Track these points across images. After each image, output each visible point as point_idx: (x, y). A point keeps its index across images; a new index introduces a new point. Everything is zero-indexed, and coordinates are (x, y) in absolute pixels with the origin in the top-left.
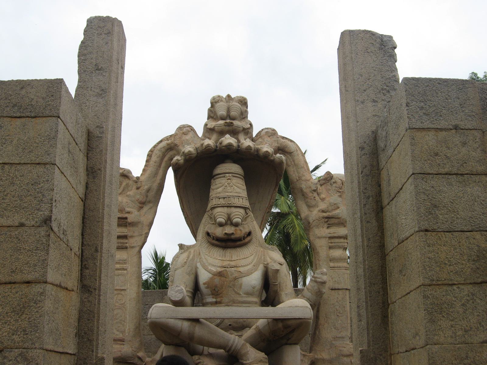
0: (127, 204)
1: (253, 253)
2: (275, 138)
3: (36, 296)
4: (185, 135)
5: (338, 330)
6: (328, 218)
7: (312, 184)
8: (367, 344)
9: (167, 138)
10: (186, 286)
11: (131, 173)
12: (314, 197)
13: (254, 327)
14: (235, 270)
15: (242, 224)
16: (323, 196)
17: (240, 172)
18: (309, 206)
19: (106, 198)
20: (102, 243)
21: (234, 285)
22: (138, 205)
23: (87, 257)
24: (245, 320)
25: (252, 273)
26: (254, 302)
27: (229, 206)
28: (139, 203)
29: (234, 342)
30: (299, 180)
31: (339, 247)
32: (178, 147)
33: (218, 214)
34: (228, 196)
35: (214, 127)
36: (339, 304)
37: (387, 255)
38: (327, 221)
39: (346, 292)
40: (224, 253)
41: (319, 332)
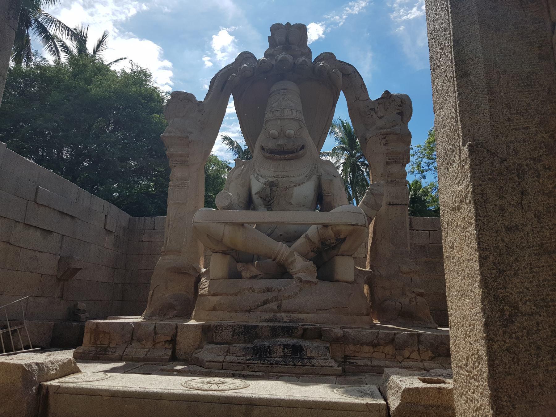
10: (239, 197)
13: (304, 235)
35: (273, 52)
38: (385, 138)
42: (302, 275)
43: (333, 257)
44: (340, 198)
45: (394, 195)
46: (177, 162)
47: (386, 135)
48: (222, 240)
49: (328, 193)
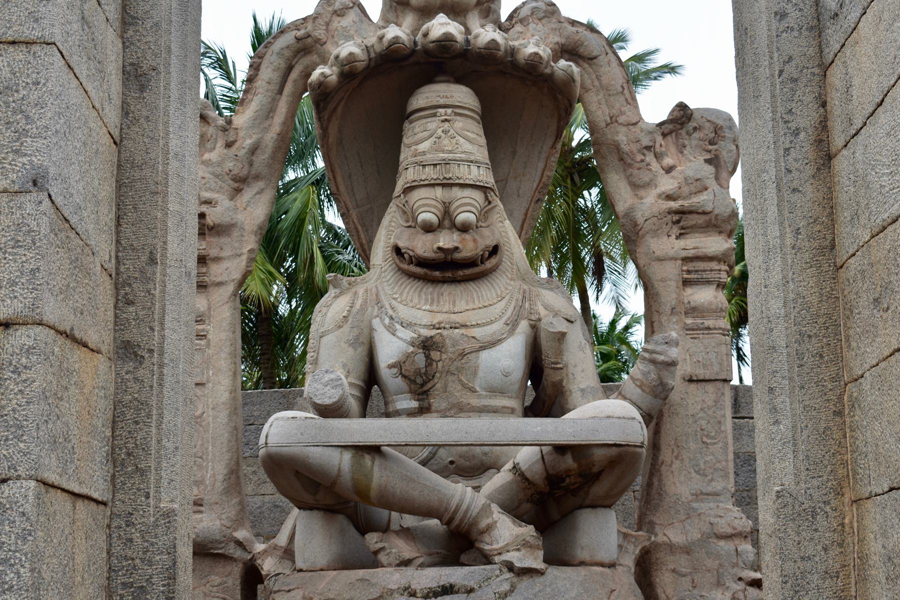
0: (204, 181)
1: (504, 295)
3: (17, 354)
4: (338, 16)
5: (706, 476)
6: (681, 212)
7: (643, 134)
8: (792, 477)
10: (348, 372)
12: (648, 164)
14: (463, 334)
16: (668, 161)
17: (473, 103)
18: (636, 186)
19: (171, 136)
20: (165, 243)
23: (129, 277)
24: (486, 449)
26: (508, 408)
27: (447, 185)
28: (232, 180)
29: (462, 501)
30: (612, 123)
31: (708, 282)
32: (322, 45)
34: (444, 160)
36: (708, 415)
37: (841, 267)
39: (724, 387)
40: (435, 296)
41: (660, 480)
42: (513, 557)
43: (573, 511)
44: (582, 371)
45: (701, 359)
47: (681, 215)
48: (334, 483)
49: (557, 363)
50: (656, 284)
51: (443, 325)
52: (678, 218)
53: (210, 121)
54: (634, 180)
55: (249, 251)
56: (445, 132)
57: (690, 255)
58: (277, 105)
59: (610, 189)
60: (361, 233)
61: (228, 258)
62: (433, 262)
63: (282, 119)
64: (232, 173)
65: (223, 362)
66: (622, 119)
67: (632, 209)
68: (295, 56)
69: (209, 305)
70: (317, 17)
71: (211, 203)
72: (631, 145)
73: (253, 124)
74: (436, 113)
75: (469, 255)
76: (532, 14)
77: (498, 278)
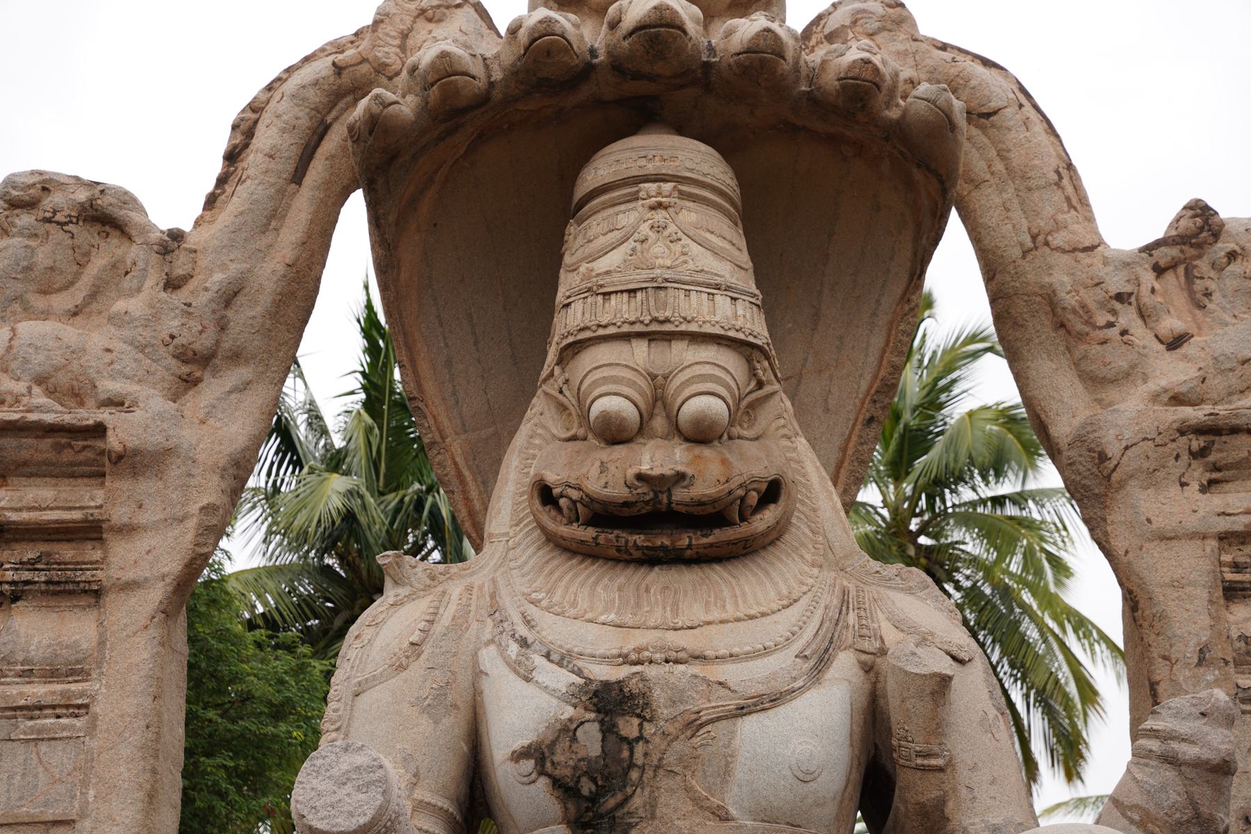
2: (900, 42)
4: (430, 20)
6: (1212, 430)
7: (1110, 269)
9: (338, 46)
11: (141, 210)
14: (696, 677)
15: (730, 438)
17: (721, 176)
18: (1095, 381)
21: (689, 762)
22: (168, 370)
25: (792, 693)
27: (659, 336)
28: (174, 356)
30: (1036, 248)
32: (390, 78)
33: (598, 375)
34: (653, 280)
44: (992, 783)
46: (26, 575)
47: (1211, 438)
49: (928, 755)
50: (1157, 592)
51: (647, 654)
52: (1202, 444)
53: (133, 233)
54: (1093, 367)
55: (202, 509)
56: (658, 229)
57: (1239, 527)
58: (289, 206)
59: (1036, 393)
60: (472, 486)
61: (155, 527)
62: (626, 512)
63: (299, 235)
64: (175, 341)
65: (122, 769)
66: (1058, 239)
67: (1091, 425)
68: (332, 105)
69: (101, 635)
70: (382, 21)
71: (122, 404)
72: (1082, 292)
73: (230, 239)
74: (638, 192)
75: (708, 492)
76: (855, 22)
77: (781, 560)
